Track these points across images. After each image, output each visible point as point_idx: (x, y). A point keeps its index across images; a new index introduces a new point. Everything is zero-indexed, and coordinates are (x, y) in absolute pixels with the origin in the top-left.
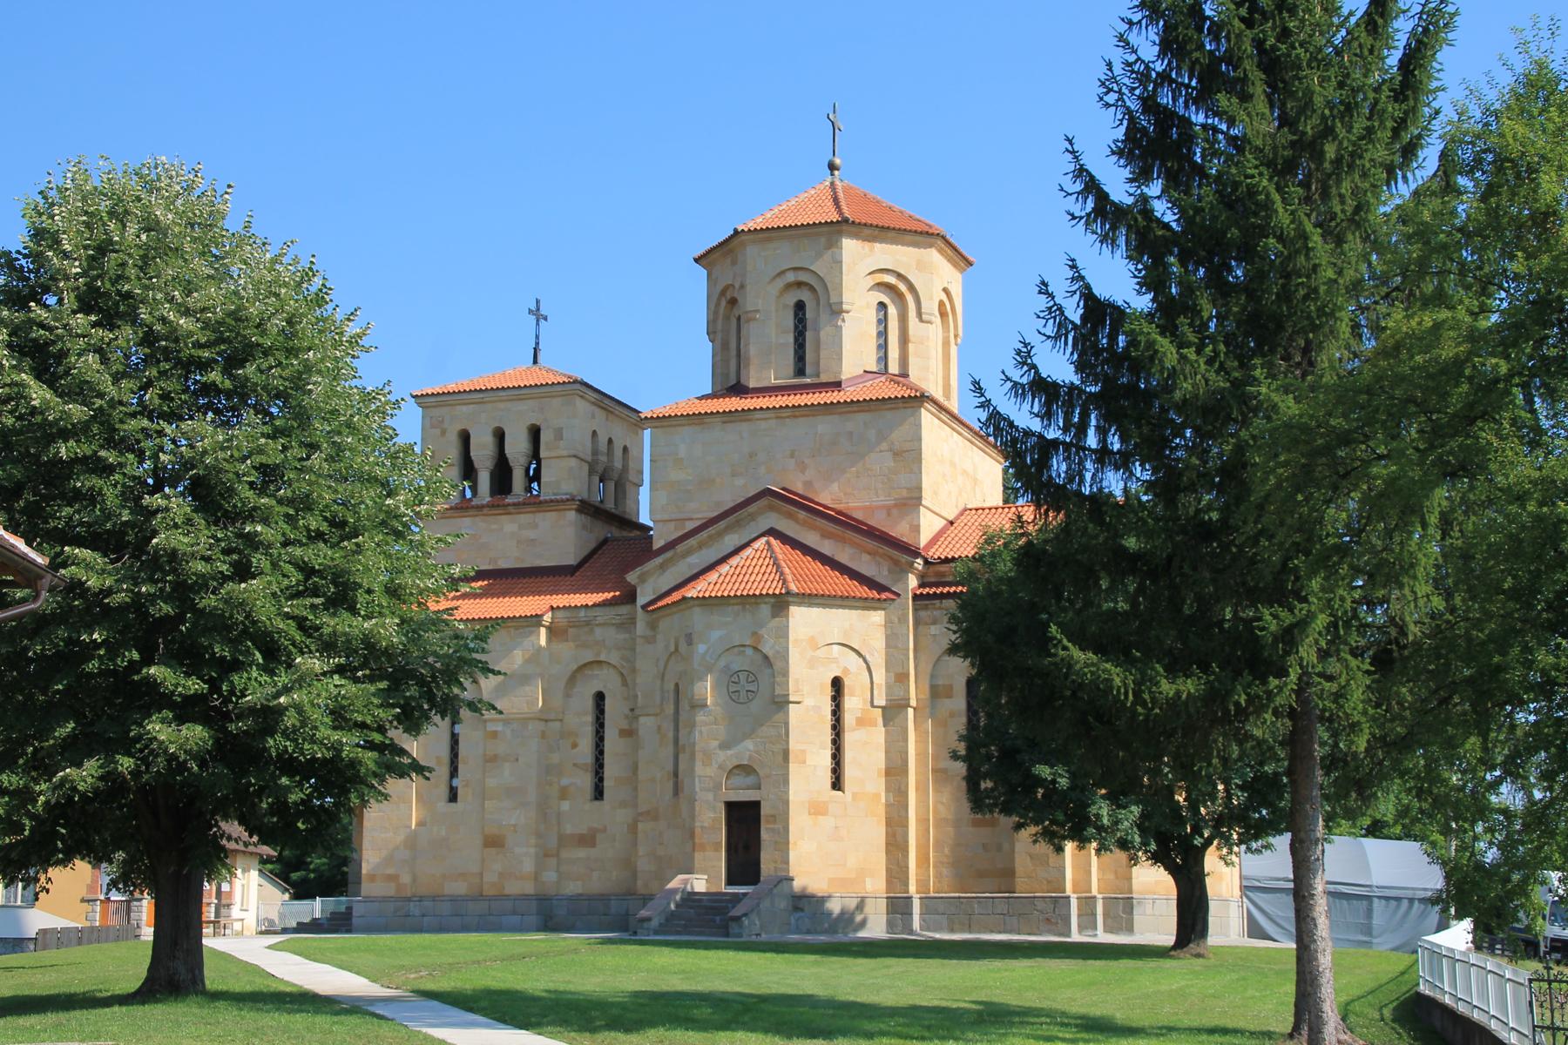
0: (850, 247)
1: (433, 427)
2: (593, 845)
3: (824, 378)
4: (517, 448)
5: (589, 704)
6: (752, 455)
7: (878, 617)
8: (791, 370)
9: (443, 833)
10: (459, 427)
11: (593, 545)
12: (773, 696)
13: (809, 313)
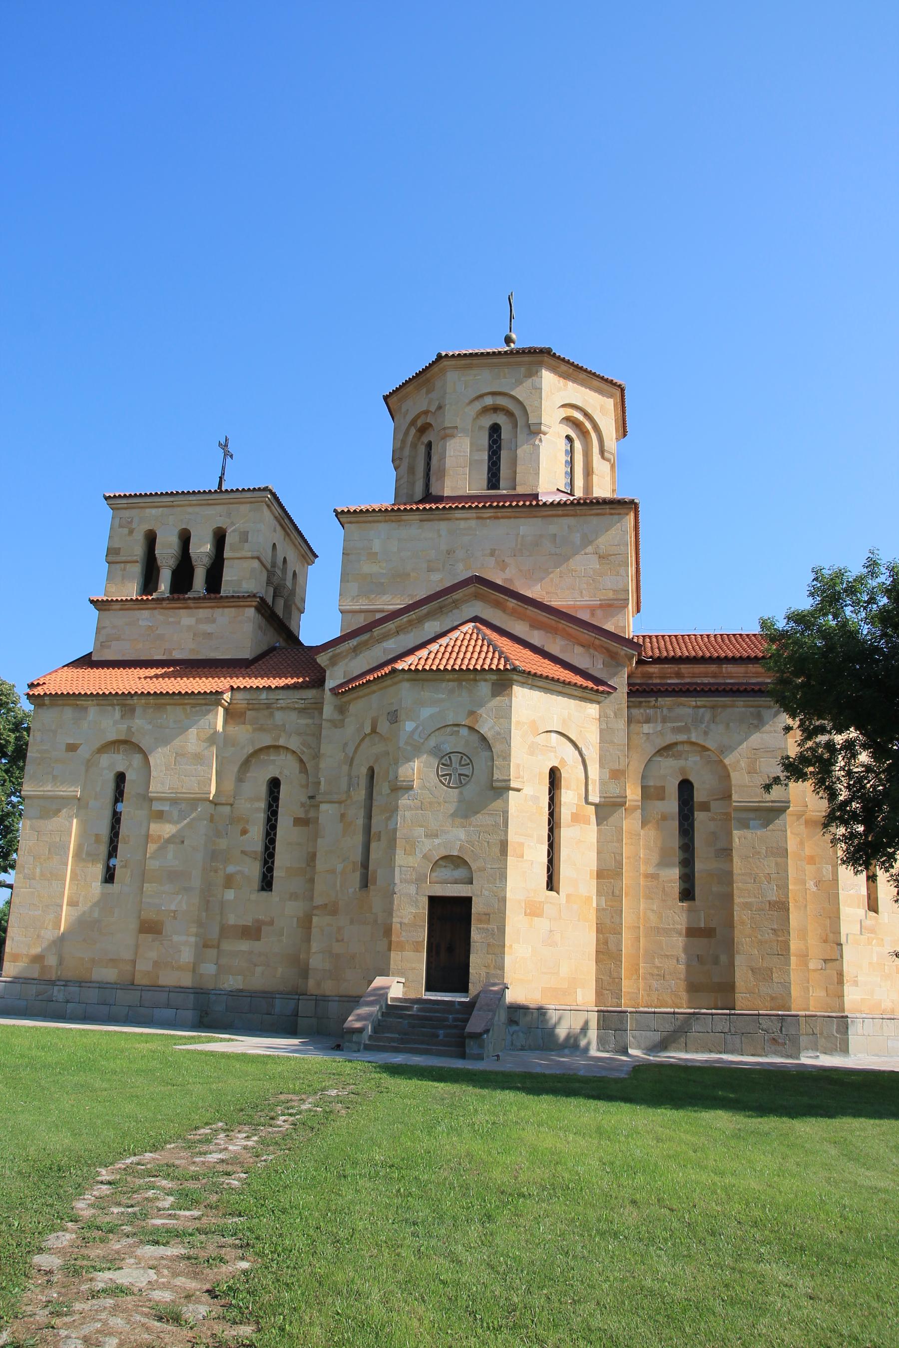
0: (548, 378)
1: (121, 526)
3: (520, 490)
4: (202, 549)
5: (263, 790)
6: (448, 553)
7: (593, 710)
8: (485, 483)
10: (146, 527)
11: (265, 648)
12: (492, 781)
13: (504, 434)
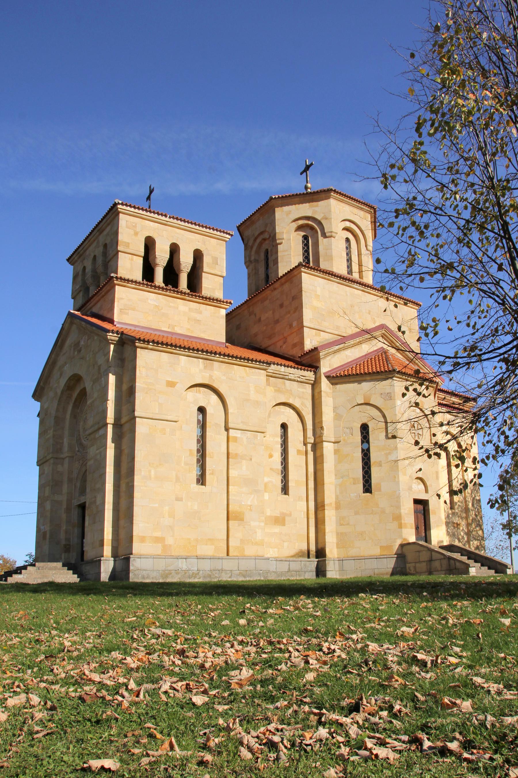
2: (284, 525)
4: (186, 261)
9: (196, 507)
